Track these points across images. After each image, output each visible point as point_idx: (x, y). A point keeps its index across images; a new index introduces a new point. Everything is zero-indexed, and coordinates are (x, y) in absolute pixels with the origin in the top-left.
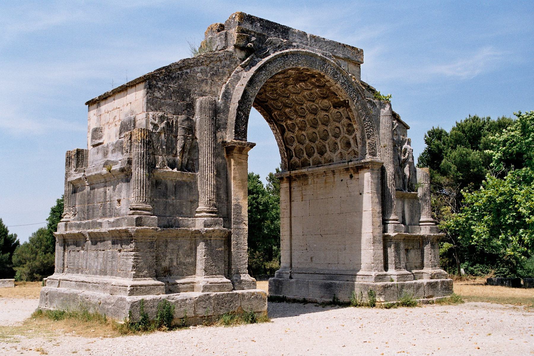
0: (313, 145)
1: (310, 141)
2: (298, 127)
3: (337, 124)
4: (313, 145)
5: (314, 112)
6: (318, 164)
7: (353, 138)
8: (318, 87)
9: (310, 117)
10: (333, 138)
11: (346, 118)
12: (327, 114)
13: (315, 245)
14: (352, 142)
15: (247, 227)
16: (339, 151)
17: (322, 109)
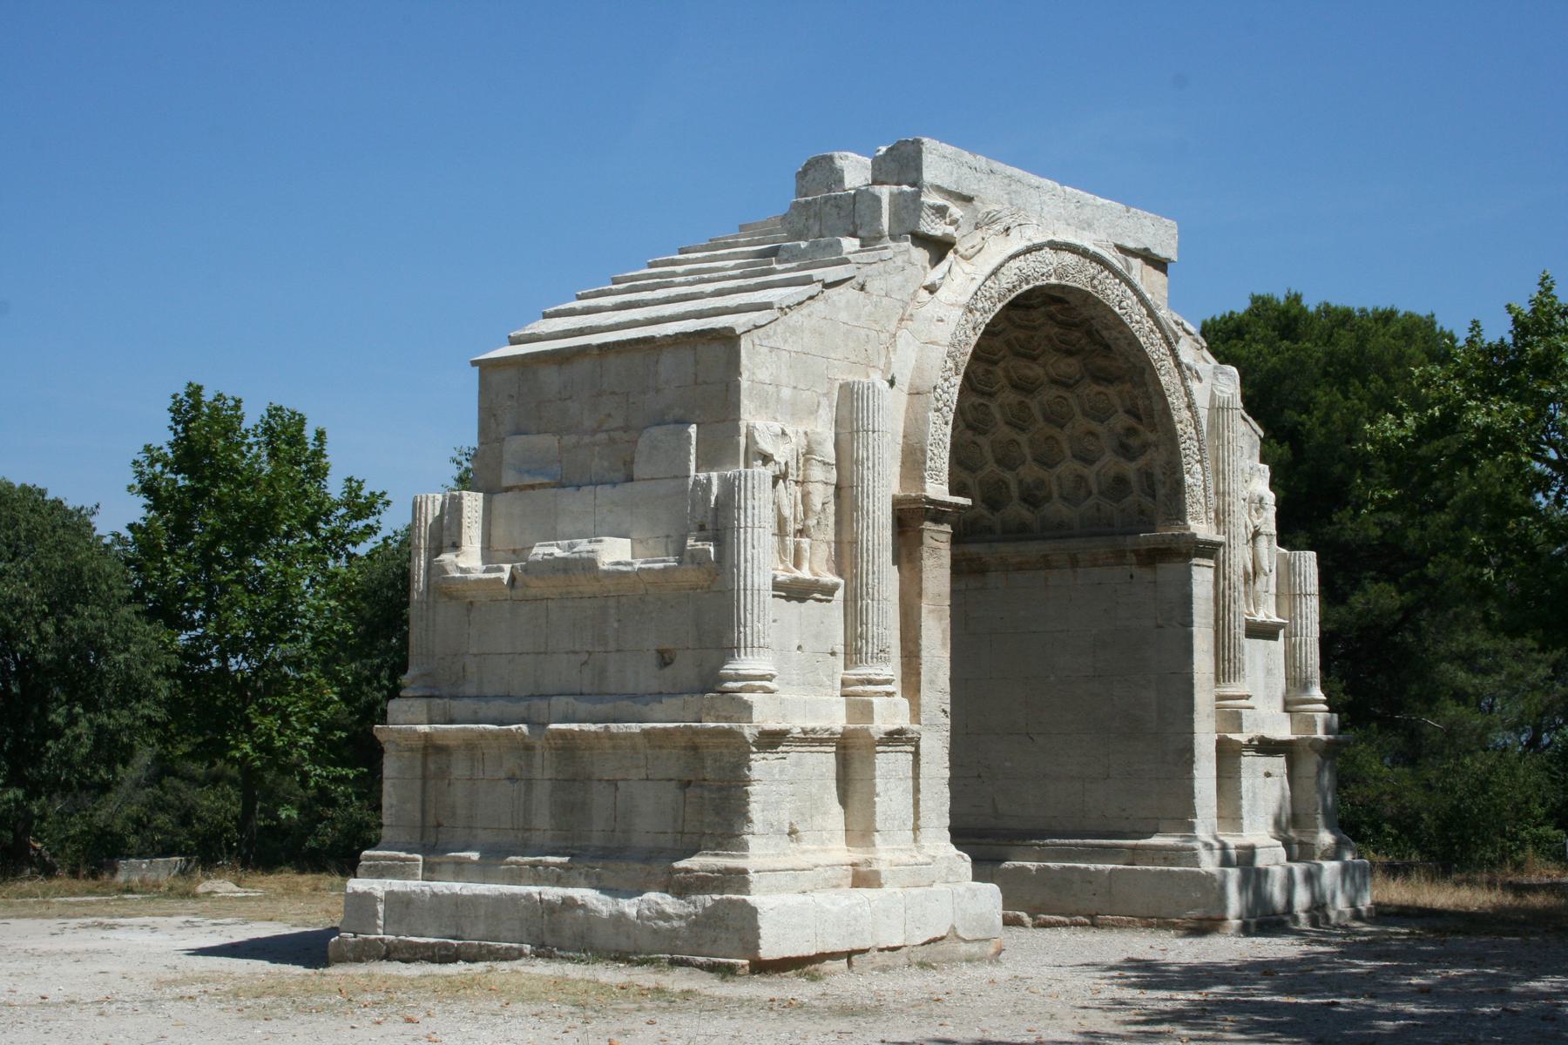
0: (1008, 476)
1: (999, 462)
2: (964, 420)
3: (1094, 426)
4: (1008, 476)
5: (1024, 387)
6: (1020, 532)
7: (1139, 470)
8: (1062, 324)
9: (1011, 397)
10: (1077, 466)
11: (1128, 412)
12: (1067, 395)
13: (1008, 764)
14: (1133, 477)
15: (948, 721)
16: (1090, 501)
17: (1054, 382)
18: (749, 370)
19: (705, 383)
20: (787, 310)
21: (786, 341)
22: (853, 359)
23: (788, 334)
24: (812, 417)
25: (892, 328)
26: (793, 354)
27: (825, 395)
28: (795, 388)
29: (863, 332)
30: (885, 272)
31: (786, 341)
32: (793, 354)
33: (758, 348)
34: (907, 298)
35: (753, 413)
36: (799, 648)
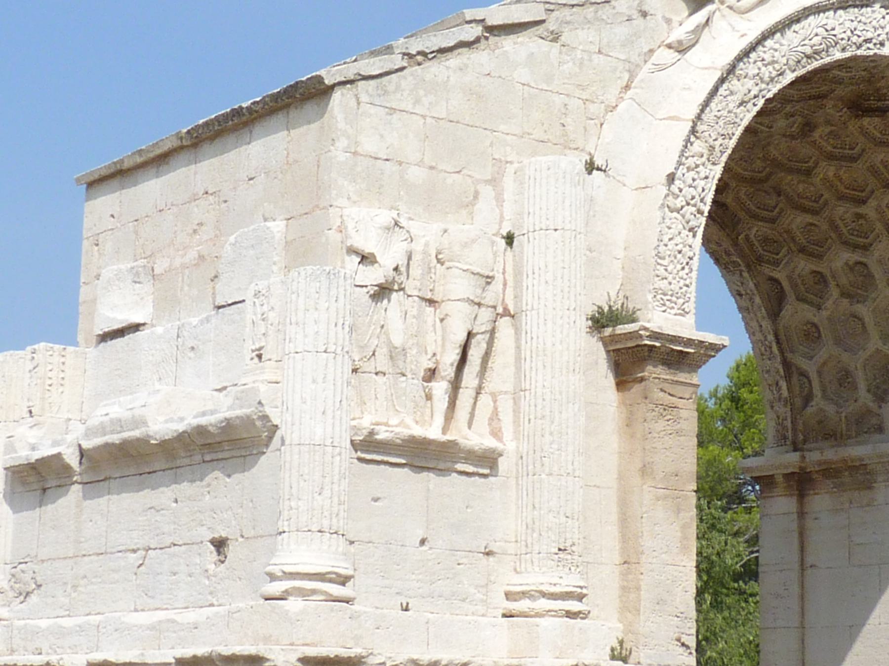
18: (348, 137)
19: (296, 161)
20: (419, 58)
21: (417, 101)
22: (538, 134)
23: (421, 92)
24: (464, 212)
25: (611, 97)
26: (429, 120)
27: (488, 182)
28: (432, 168)
29: (558, 100)
30: (597, 19)
31: (417, 101)
32: (429, 120)
33: (364, 107)
34: (635, 58)
35: (354, 198)
36: (423, 542)
